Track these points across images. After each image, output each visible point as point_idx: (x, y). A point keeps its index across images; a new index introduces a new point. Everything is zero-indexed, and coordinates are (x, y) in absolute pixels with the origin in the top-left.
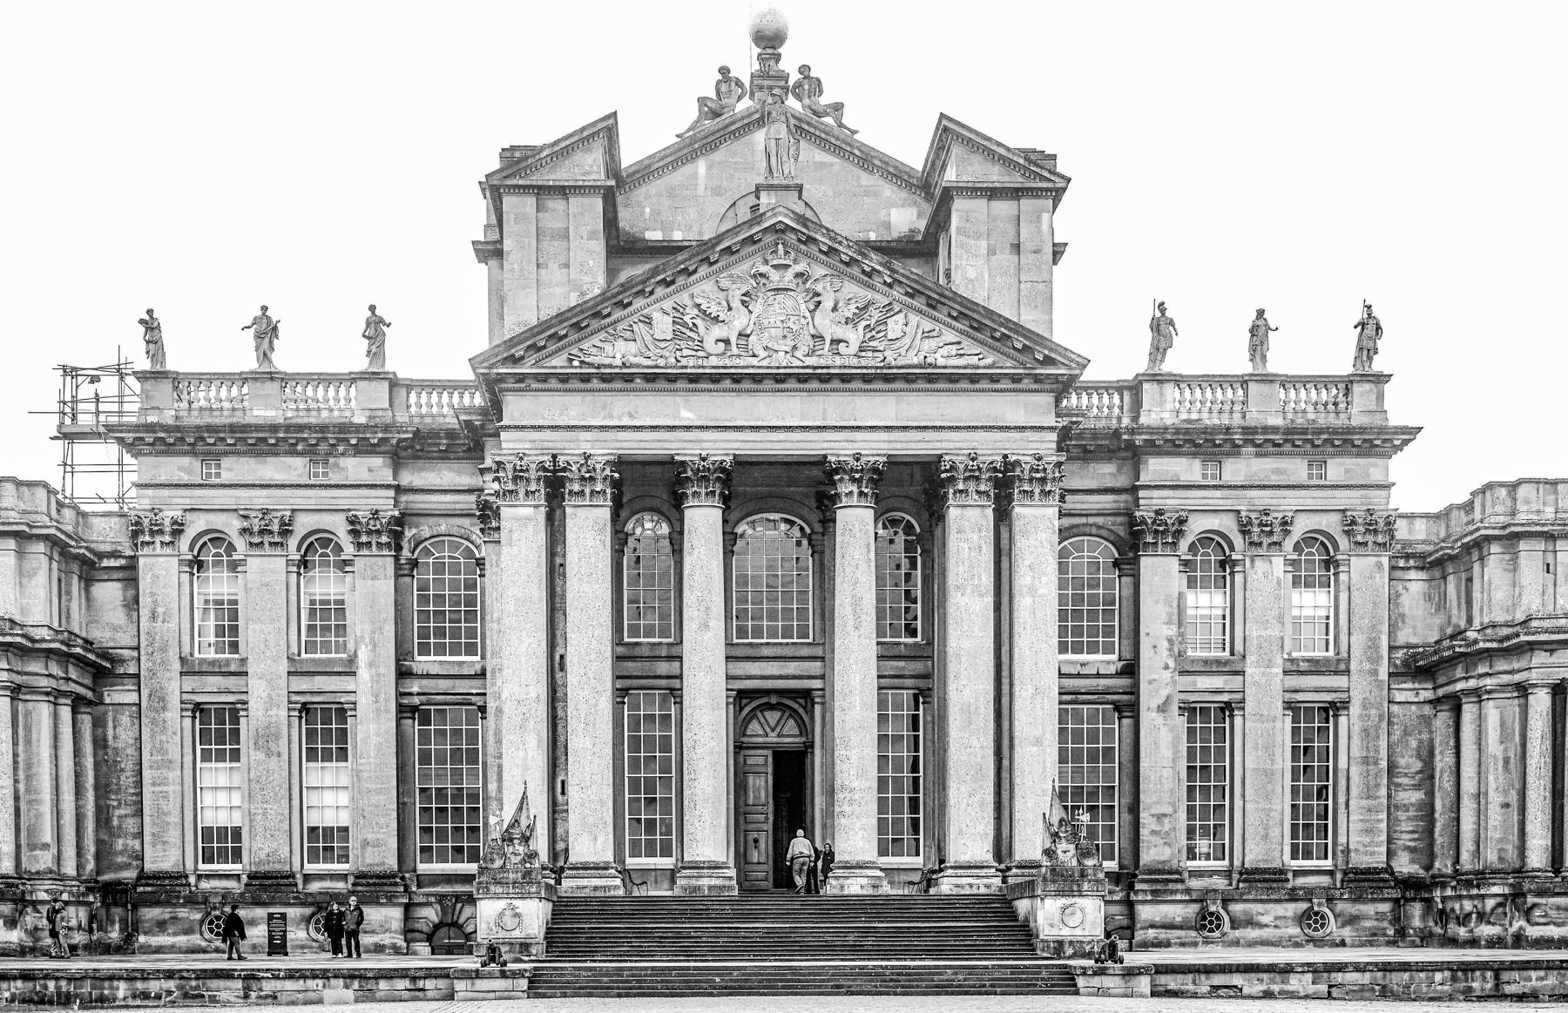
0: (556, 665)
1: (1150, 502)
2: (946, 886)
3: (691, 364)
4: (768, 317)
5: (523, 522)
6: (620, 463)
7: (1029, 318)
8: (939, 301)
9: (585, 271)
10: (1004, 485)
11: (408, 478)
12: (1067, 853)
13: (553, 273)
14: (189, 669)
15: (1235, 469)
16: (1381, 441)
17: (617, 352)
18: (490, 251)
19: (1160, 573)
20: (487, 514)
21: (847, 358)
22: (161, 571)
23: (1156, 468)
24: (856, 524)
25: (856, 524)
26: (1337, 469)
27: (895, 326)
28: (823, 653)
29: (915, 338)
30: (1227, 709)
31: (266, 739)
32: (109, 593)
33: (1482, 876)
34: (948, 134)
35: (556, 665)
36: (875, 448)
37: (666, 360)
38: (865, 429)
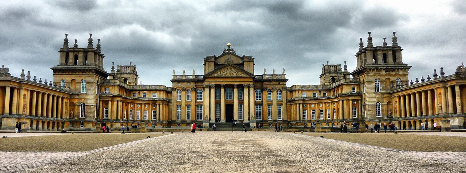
0: (210, 102)
1: (264, 86)
2: (244, 122)
3: (222, 76)
4: (228, 72)
5: (207, 90)
6: (215, 85)
7: (251, 72)
8: (243, 71)
9: (212, 68)
10: (249, 87)
11: (197, 84)
12: (253, 119)
13: (210, 68)
14: (177, 102)
15: (272, 83)
16: (286, 81)
17: (215, 75)
18: (204, 65)
19: (265, 93)
20: (204, 88)
21: (235, 76)
22: (174, 93)
23: (265, 83)
24: (236, 90)
25: (236, 90)
26: (281, 83)
27: (239, 73)
28: (233, 101)
29: (241, 74)
30: (271, 105)
31: (183, 108)
32: (169, 94)
33: (294, 121)
34: (244, 56)
35: (210, 102)
36: (238, 83)
37: (219, 76)
38: (237, 82)
